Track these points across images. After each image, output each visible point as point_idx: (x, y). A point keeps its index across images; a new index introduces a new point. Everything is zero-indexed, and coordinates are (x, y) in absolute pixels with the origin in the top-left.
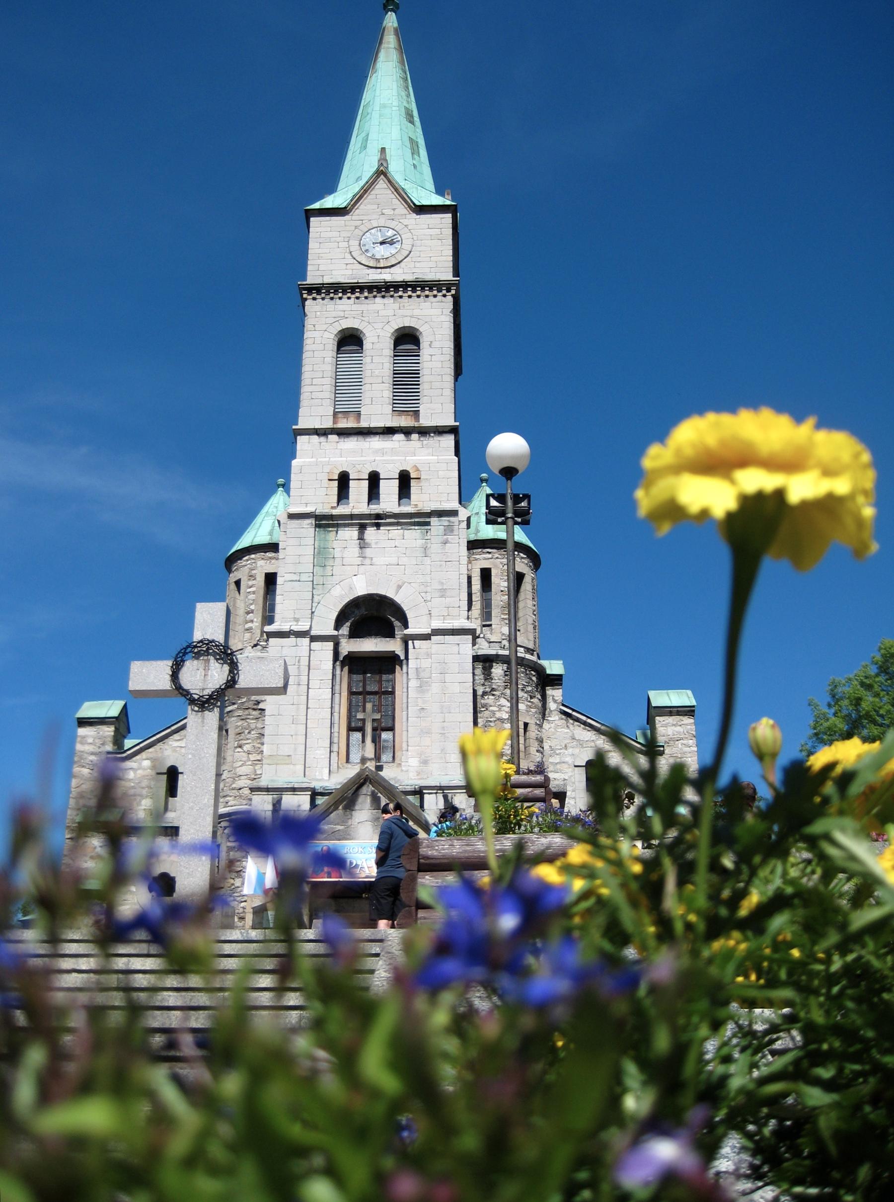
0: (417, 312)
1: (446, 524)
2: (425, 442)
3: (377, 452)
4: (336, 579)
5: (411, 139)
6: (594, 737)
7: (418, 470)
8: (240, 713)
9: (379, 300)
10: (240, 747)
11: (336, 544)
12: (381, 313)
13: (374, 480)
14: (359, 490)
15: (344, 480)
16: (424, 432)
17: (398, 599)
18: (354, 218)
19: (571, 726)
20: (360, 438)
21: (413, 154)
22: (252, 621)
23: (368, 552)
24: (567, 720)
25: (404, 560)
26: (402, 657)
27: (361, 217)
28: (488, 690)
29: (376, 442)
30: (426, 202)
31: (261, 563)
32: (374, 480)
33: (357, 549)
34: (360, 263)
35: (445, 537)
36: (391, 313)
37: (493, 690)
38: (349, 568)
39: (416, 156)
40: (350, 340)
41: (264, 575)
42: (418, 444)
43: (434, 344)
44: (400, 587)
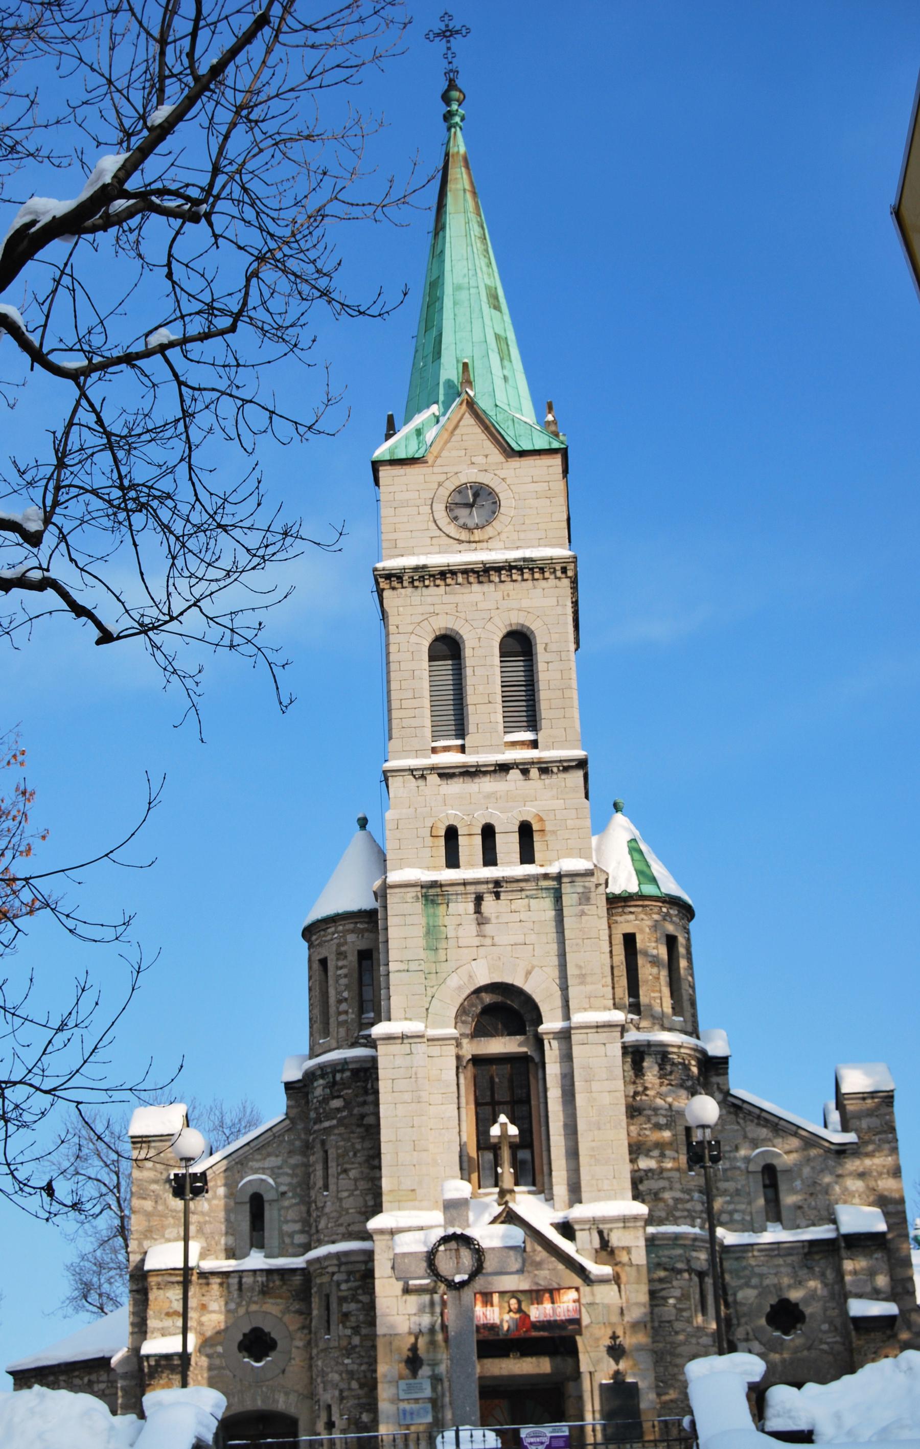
0: (525, 603)
1: (580, 890)
2: (547, 781)
3: (488, 796)
4: (451, 965)
5: (497, 337)
6: (770, 1135)
7: (541, 820)
8: (342, 1130)
9: (476, 587)
10: (345, 1171)
11: (447, 921)
12: (480, 606)
13: (488, 832)
14: (470, 846)
15: (452, 834)
16: (545, 769)
17: (528, 988)
18: (436, 470)
19: (741, 1121)
20: (467, 779)
21: (502, 360)
22: (346, 1012)
23: (488, 929)
24: (737, 1115)
25: (531, 938)
26: (537, 1059)
27: (445, 469)
28: (640, 1089)
29: (487, 784)
30: (527, 446)
31: (351, 938)
32: (488, 832)
33: (473, 928)
34: (448, 536)
35: (581, 907)
36: (492, 605)
37: (646, 1089)
38: (466, 951)
39: (506, 363)
40: (448, 648)
41: (356, 953)
42: (540, 783)
43: (552, 647)
44: (528, 973)
